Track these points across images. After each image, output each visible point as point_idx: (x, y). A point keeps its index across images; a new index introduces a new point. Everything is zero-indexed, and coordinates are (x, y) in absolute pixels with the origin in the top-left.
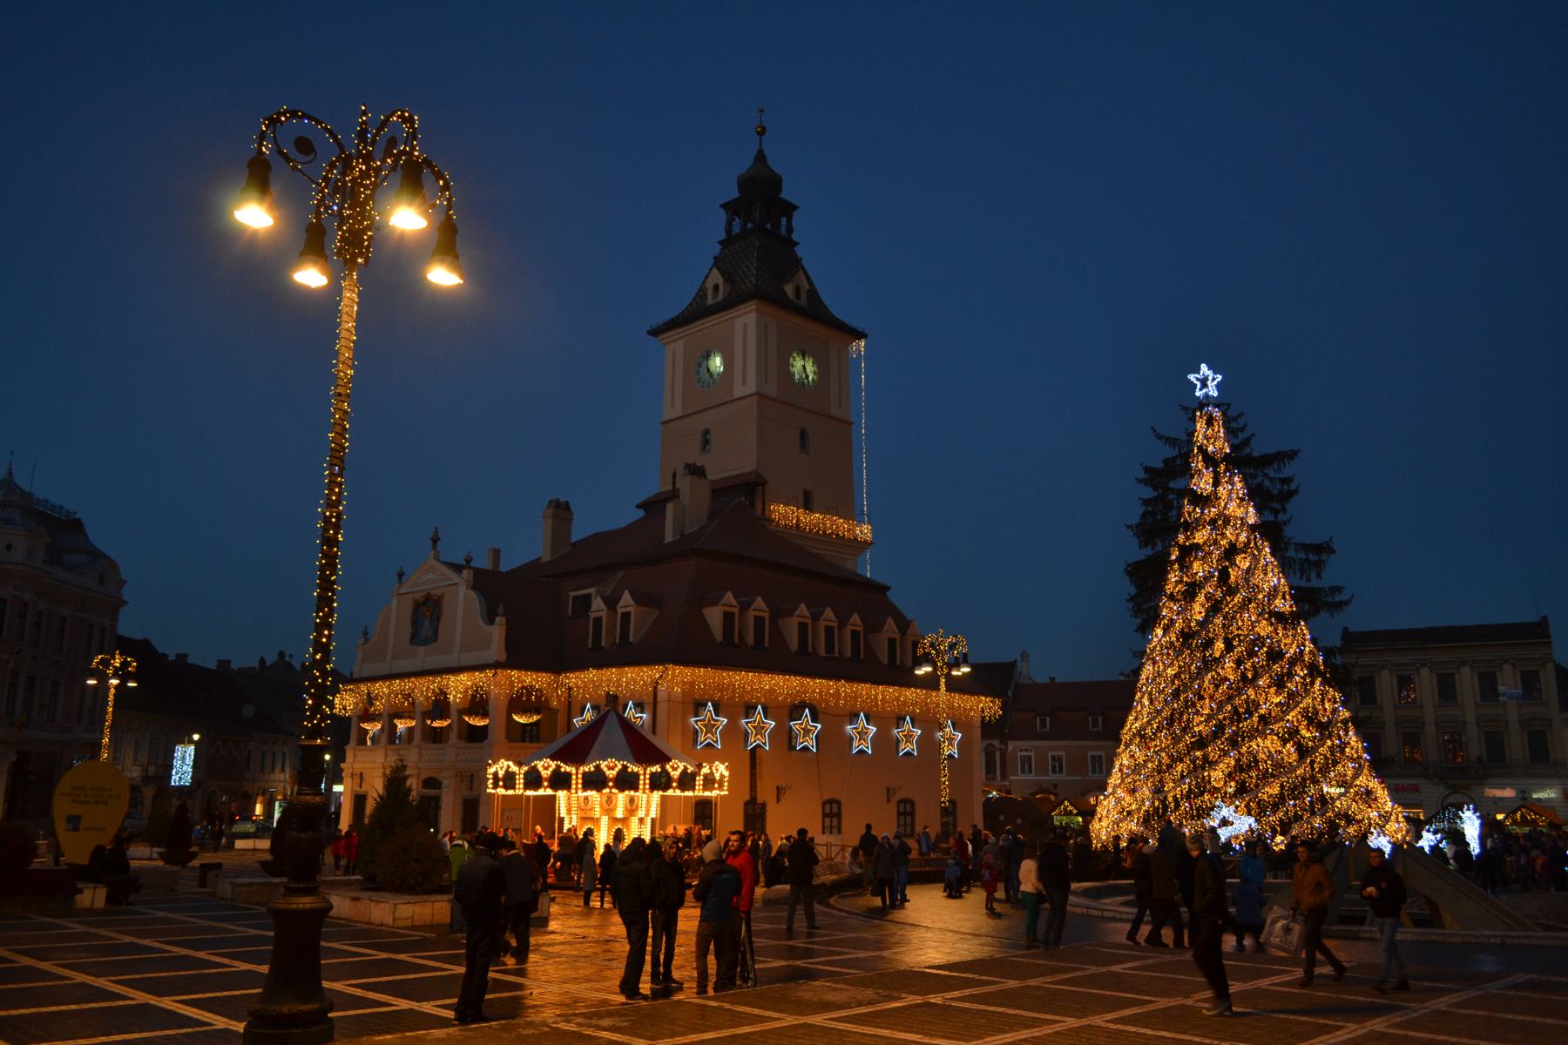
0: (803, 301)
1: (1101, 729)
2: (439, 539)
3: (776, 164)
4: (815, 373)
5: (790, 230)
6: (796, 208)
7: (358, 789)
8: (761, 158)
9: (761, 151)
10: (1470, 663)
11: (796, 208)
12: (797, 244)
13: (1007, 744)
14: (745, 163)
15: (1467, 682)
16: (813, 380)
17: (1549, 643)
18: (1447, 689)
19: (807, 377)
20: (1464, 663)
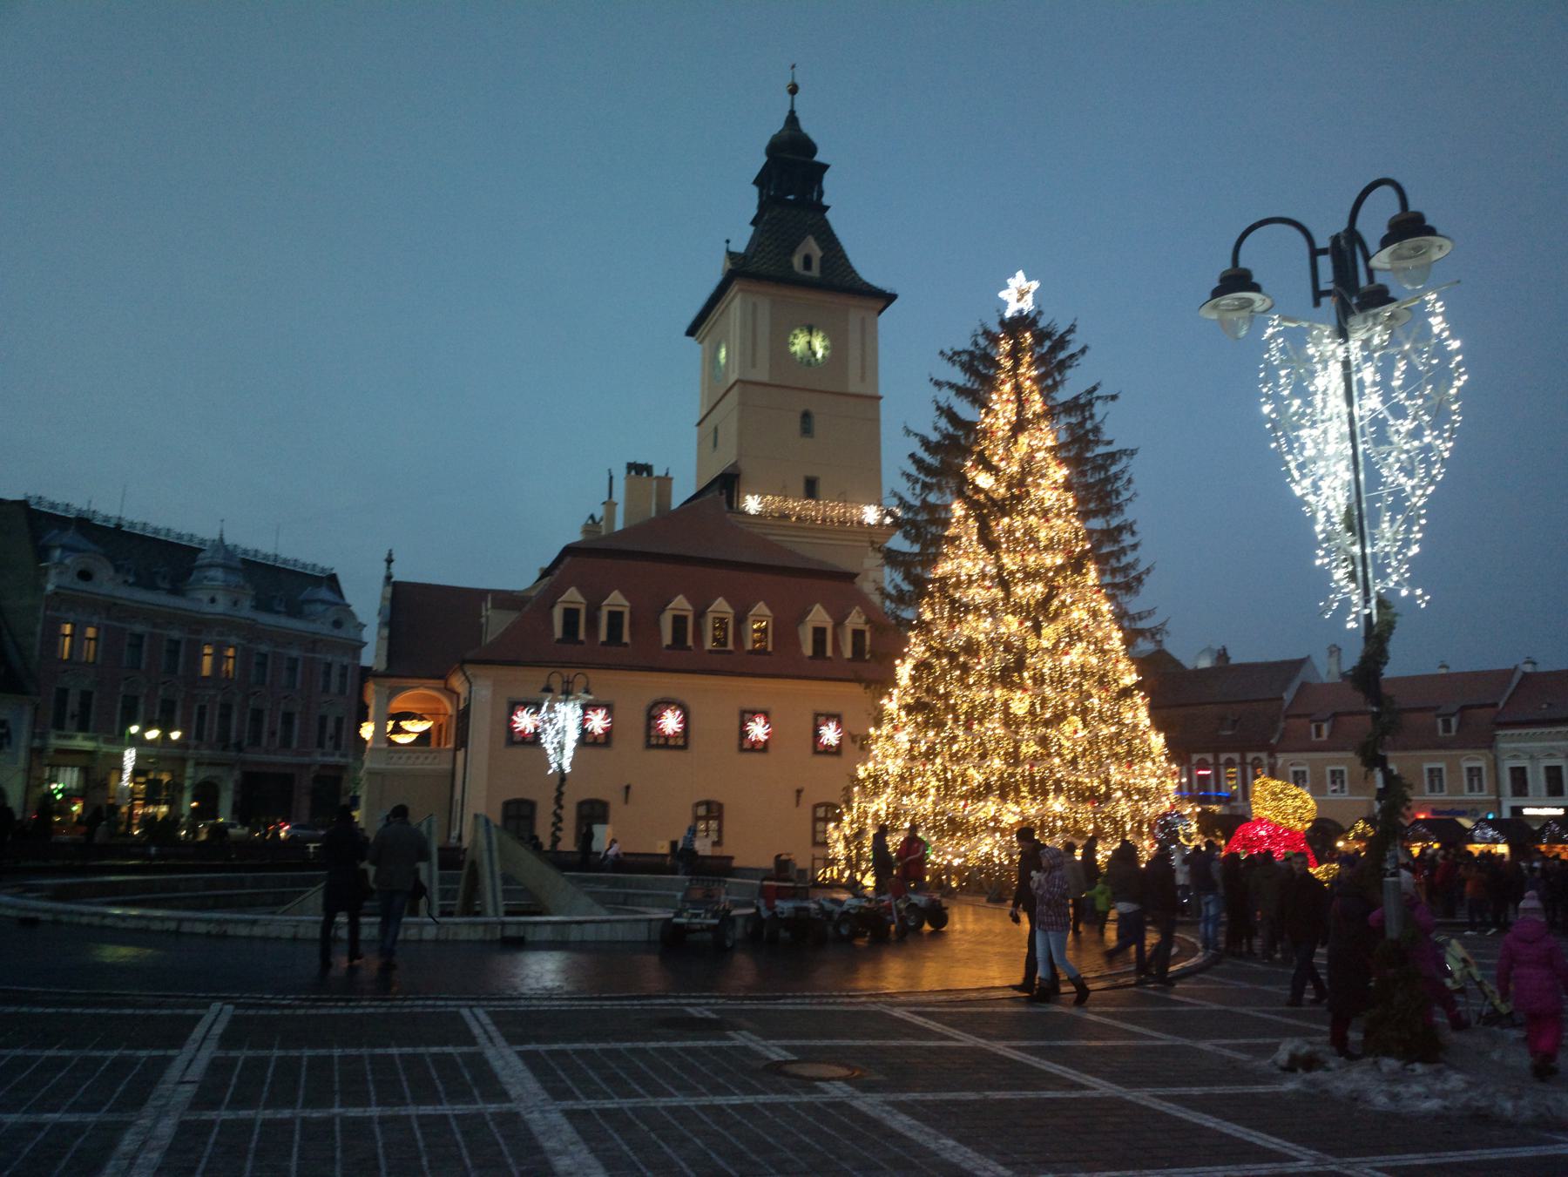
0: (815, 272)
1: (1453, 733)
3: (807, 126)
4: (826, 348)
5: (821, 194)
8: (792, 119)
9: (792, 112)
12: (827, 208)
13: (1275, 758)
16: (823, 356)
19: (814, 354)
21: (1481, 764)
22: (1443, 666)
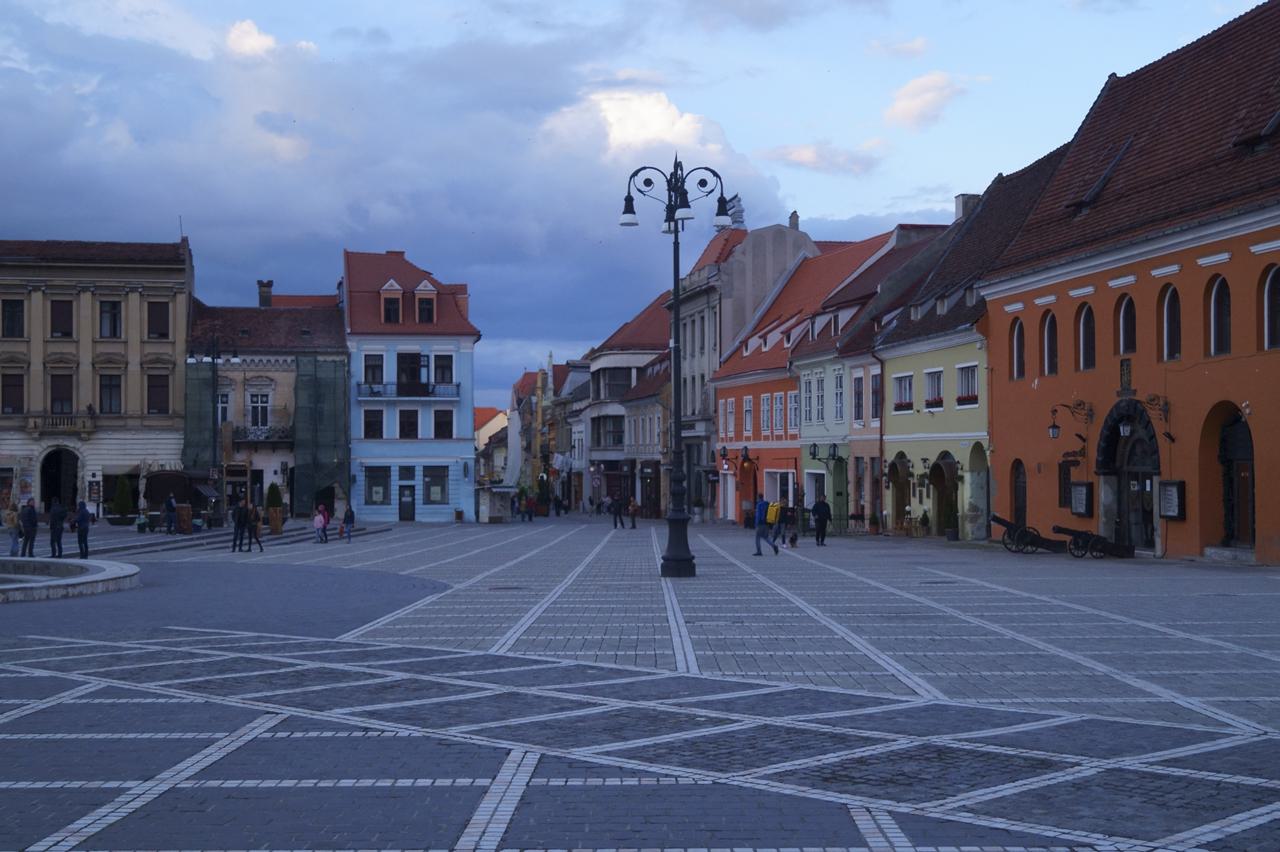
10: (92, 289)
15: (86, 311)
18: (62, 322)
20: (85, 289)
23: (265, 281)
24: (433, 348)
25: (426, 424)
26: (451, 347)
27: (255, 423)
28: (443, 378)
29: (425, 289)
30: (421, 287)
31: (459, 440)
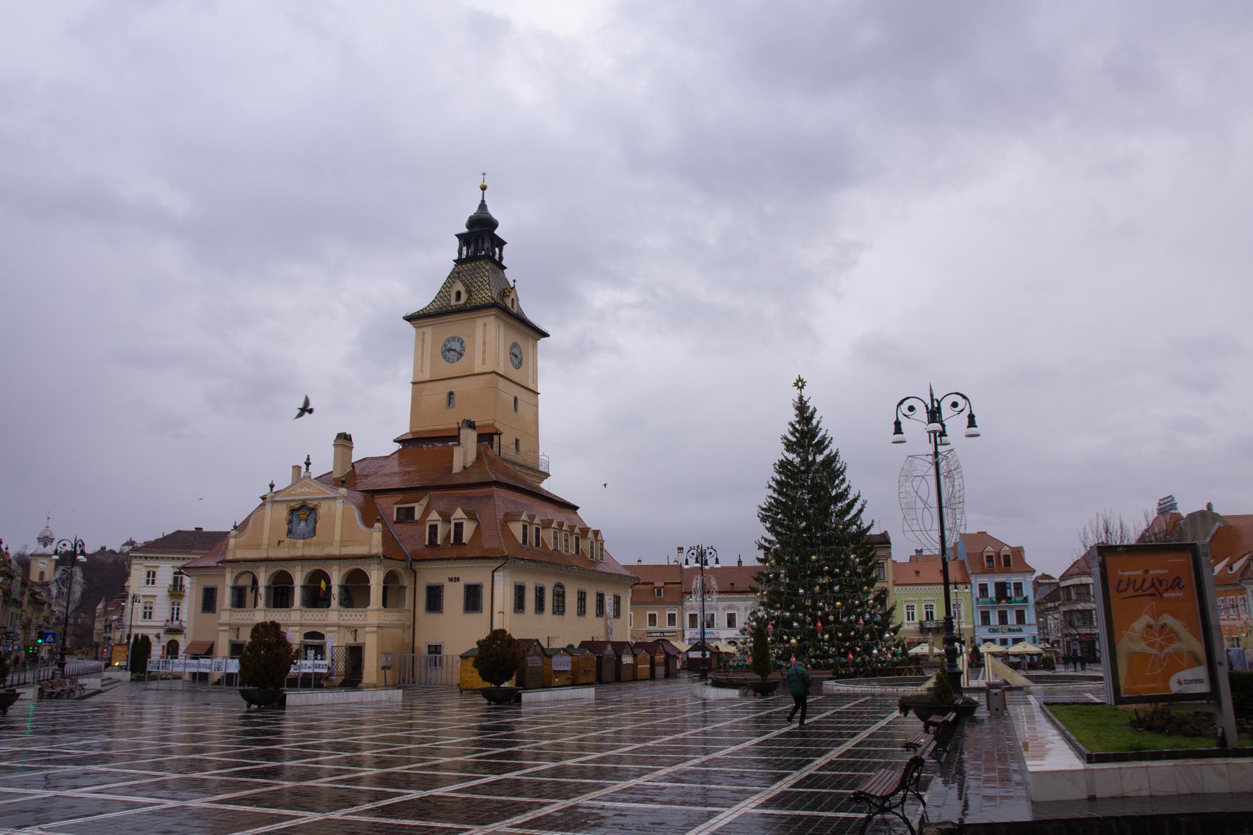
2: (310, 464)
3: (494, 212)
6: (505, 243)
7: (234, 639)
8: (483, 206)
9: (483, 201)
11: (505, 243)
14: (473, 210)
17: (890, 547)
21: (676, 612)
22: (640, 561)
23: (919, 549)
24: (1012, 579)
25: (1012, 618)
26: (1021, 578)
27: (927, 619)
28: (983, 595)
29: (1005, 551)
30: (1003, 549)
31: (1029, 625)
